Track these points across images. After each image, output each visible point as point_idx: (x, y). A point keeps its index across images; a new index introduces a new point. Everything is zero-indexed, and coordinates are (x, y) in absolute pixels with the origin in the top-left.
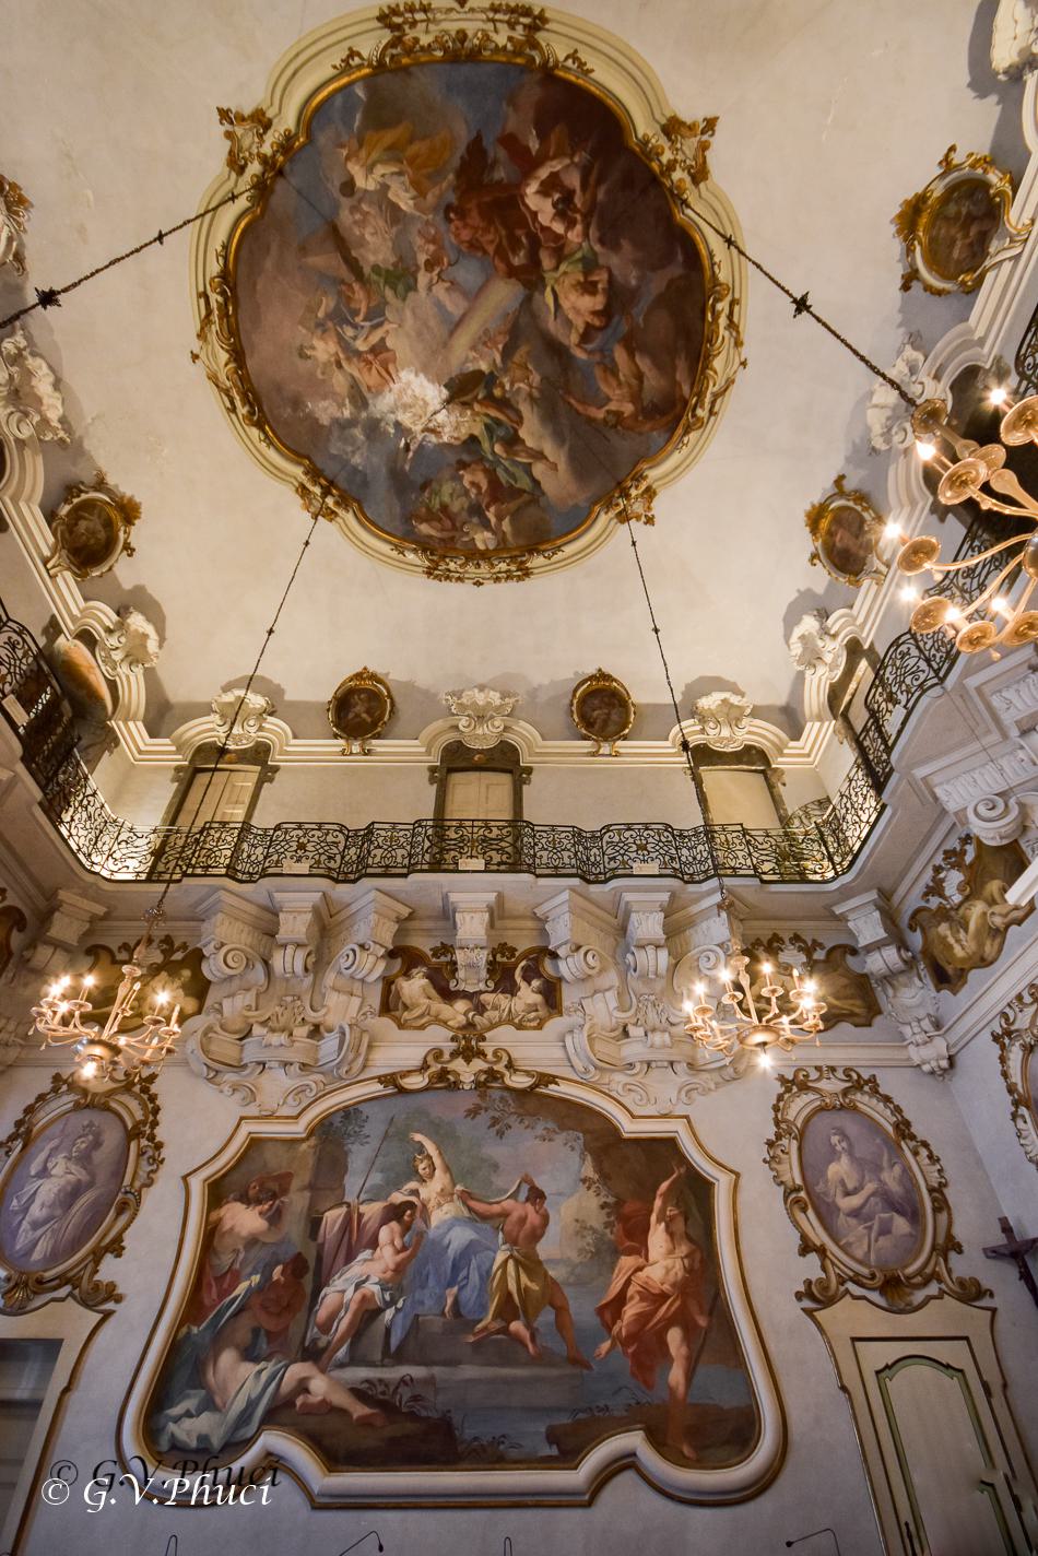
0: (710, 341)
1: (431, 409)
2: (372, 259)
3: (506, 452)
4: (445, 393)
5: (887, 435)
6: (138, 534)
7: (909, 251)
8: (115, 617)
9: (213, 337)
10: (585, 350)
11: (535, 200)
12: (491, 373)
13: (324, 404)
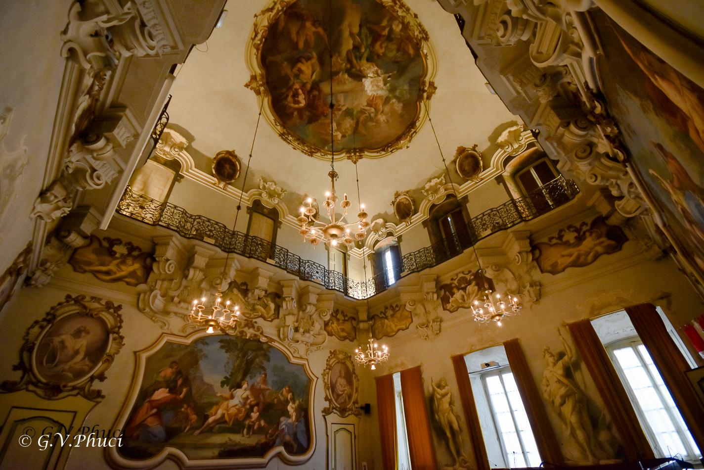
1: (371, 80)
2: (352, 122)
3: (361, 46)
4: (364, 80)
6: (469, 145)
8: (500, 150)
9: (400, 145)
10: (312, 54)
11: (303, 104)
12: (346, 72)
13: (396, 108)
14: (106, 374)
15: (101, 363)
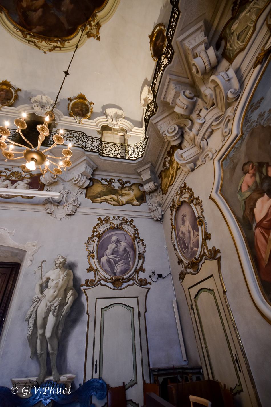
0: (49, 40)
5: (35, 102)
7: (76, 98)
14: (208, 231)
15: (200, 228)
